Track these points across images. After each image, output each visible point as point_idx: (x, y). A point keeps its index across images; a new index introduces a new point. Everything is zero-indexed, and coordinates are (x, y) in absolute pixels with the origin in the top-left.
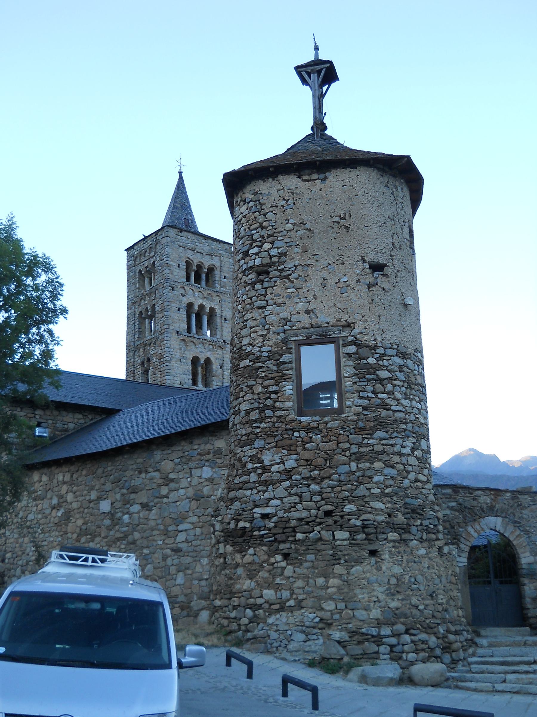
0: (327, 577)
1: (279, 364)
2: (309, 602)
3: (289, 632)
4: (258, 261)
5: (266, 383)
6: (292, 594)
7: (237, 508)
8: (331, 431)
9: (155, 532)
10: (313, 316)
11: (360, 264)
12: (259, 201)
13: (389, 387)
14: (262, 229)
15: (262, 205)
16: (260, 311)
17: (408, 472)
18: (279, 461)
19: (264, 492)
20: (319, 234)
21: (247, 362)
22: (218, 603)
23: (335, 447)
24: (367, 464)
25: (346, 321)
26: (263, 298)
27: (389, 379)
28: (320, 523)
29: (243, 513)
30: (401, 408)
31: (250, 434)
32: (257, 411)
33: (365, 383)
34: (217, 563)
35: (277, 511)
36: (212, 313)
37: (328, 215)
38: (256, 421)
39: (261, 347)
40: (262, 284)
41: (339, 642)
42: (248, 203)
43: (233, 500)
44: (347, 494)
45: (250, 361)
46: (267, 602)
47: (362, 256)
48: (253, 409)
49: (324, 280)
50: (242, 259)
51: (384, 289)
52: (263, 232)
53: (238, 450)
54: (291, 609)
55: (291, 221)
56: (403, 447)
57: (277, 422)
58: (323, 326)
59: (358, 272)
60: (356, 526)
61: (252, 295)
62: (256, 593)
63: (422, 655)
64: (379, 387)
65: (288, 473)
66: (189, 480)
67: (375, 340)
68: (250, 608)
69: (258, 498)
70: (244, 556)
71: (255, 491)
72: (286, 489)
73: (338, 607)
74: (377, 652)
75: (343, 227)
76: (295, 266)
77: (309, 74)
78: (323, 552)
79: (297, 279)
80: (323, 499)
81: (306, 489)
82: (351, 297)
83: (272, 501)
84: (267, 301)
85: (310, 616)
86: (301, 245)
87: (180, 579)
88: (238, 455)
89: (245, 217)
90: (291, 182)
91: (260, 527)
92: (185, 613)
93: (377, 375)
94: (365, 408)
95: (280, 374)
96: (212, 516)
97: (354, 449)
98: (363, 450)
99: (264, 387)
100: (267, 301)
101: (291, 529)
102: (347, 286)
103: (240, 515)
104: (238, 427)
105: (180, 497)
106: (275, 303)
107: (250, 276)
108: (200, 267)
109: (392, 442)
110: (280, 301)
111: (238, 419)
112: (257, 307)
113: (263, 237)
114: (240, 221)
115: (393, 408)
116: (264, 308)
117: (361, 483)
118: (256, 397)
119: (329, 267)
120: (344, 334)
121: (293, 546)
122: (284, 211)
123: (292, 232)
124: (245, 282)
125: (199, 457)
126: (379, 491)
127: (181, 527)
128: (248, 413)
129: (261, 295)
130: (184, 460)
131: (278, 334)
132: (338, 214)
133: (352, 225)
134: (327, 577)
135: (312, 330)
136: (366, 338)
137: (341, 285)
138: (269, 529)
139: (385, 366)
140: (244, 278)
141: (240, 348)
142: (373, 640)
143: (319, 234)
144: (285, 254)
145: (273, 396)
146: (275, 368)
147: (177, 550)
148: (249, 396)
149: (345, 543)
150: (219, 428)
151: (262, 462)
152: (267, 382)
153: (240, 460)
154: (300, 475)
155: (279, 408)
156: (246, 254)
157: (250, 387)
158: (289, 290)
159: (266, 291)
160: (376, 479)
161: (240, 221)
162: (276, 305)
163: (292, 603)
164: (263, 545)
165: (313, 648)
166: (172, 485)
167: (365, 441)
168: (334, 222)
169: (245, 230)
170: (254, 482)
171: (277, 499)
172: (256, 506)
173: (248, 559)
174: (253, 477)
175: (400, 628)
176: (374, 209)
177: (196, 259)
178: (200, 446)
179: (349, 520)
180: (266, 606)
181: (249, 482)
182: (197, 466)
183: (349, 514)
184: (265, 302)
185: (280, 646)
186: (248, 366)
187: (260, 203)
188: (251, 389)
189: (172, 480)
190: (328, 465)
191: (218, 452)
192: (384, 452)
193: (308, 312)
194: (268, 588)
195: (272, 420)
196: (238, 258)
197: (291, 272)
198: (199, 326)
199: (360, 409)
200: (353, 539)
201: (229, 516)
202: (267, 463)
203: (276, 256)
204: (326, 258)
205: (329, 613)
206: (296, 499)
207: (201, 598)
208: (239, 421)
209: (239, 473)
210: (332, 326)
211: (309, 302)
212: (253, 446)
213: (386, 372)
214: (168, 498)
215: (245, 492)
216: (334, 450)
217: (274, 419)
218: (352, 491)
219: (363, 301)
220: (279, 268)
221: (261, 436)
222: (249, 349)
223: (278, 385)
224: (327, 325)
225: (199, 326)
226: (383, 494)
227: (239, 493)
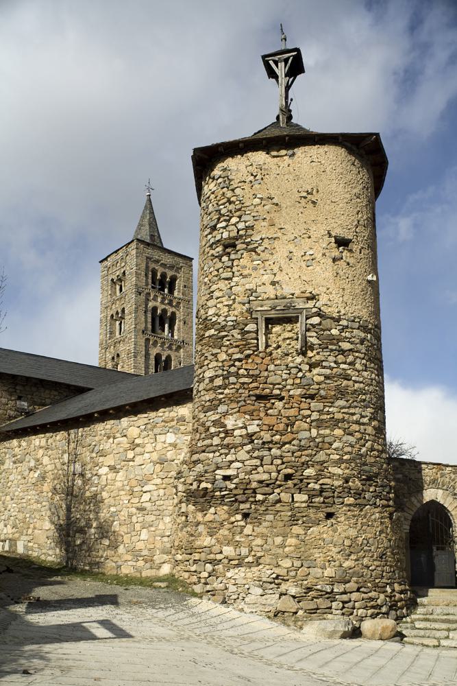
0: (285, 536)
1: (243, 333)
2: (267, 559)
3: (247, 586)
4: (225, 235)
5: (230, 351)
6: (250, 551)
7: (199, 470)
8: (293, 398)
9: (122, 493)
11: (326, 238)
12: (228, 177)
14: (230, 204)
15: (230, 180)
16: (227, 282)
18: (241, 425)
19: (226, 455)
20: (286, 208)
21: (212, 332)
22: (179, 557)
23: (297, 414)
24: (328, 431)
25: (311, 293)
26: (229, 270)
27: (350, 350)
28: (280, 486)
29: (206, 475)
30: (361, 379)
31: (213, 400)
32: (221, 378)
33: (328, 353)
34: (178, 521)
35: (238, 474)
37: (295, 190)
38: (219, 387)
39: (226, 317)
40: (229, 257)
41: (294, 597)
42: (217, 180)
43: (196, 462)
44: (308, 459)
45: (216, 330)
46: (226, 558)
48: (217, 376)
50: (209, 234)
51: (348, 264)
52: (231, 207)
53: (202, 415)
54: (250, 565)
55: (258, 196)
56: (362, 417)
57: (240, 388)
59: (324, 246)
60: (314, 490)
62: (216, 549)
63: (370, 612)
64: (341, 358)
65: (250, 437)
66: (154, 445)
67: (339, 312)
68: (210, 563)
69: (219, 460)
70: (206, 514)
71: (217, 454)
72: (248, 452)
73: (295, 565)
74: (331, 608)
75: (310, 202)
76: (261, 239)
77: (276, 63)
78: (282, 513)
79: (263, 251)
80: (283, 463)
81: (267, 453)
82: (316, 270)
83: (234, 464)
84: (233, 273)
85: (266, 572)
86: (268, 218)
87: (144, 535)
88: (201, 421)
89: (213, 193)
90: (259, 157)
91: (222, 488)
92: (148, 565)
93: (340, 347)
94: (327, 377)
95: (245, 342)
96: (175, 478)
97: (315, 416)
98: (325, 417)
101: (252, 490)
102: (312, 260)
103: (202, 476)
104: (202, 393)
105: (145, 462)
107: (217, 250)
109: (352, 411)
110: (245, 272)
111: (202, 386)
112: (223, 279)
114: (209, 197)
115: (353, 378)
116: (230, 279)
117: (322, 449)
118: (220, 364)
120: (307, 306)
121: (253, 506)
123: (259, 208)
124: (213, 255)
125: (163, 424)
126: (338, 457)
127: (144, 489)
128: (212, 380)
129: (228, 267)
130: (149, 426)
131: (244, 304)
132: (306, 190)
133: (319, 200)
134: (285, 536)
135: (276, 301)
136: (330, 309)
137: (307, 259)
138: (231, 490)
139: (348, 338)
140: (212, 252)
141: (206, 318)
142: (327, 596)
143: (286, 208)
144: (252, 228)
146: (239, 337)
147: (141, 509)
148: (214, 364)
149: (304, 505)
150: (182, 397)
151: (225, 426)
152: (232, 350)
153: (203, 425)
154: (262, 439)
156: (214, 228)
157: (215, 355)
158: (255, 263)
159: (233, 264)
160: (335, 445)
161: (209, 197)
163: (250, 559)
164: (223, 505)
165: (269, 602)
166: (138, 450)
167: (327, 409)
168: (301, 197)
169: (213, 205)
170: (217, 445)
171: (238, 461)
172: (218, 468)
173: (209, 517)
174: (216, 441)
175: (352, 585)
176: (341, 186)
178: (164, 413)
179: (309, 483)
180: (226, 561)
181: (212, 445)
182: (162, 432)
183: (308, 477)
184: (231, 273)
185: (238, 598)
186: (213, 335)
188: (216, 357)
189: (138, 445)
190: (289, 430)
191: (182, 420)
192: (343, 420)
193: (273, 283)
194: (228, 544)
195: (236, 386)
196: (206, 233)
199: (322, 378)
200: (311, 502)
201: (192, 477)
202: (229, 427)
203: (243, 229)
204: (293, 231)
205: (286, 570)
206: (257, 462)
207: (163, 552)
208: (203, 388)
209: (202, 437)
210: (297, 298)
213: (349, 344)
214: (134, 461)
215: (208, 454)
216: (295, 417)
217: (237, 386)
218: (311, 455)
219: (328, 274)
220: (246, 241)
221: (225, 402)
222: (214, 319)
223: (242, 353)
224: (291, 296)
226: (341, 461)
227: (202, 456)
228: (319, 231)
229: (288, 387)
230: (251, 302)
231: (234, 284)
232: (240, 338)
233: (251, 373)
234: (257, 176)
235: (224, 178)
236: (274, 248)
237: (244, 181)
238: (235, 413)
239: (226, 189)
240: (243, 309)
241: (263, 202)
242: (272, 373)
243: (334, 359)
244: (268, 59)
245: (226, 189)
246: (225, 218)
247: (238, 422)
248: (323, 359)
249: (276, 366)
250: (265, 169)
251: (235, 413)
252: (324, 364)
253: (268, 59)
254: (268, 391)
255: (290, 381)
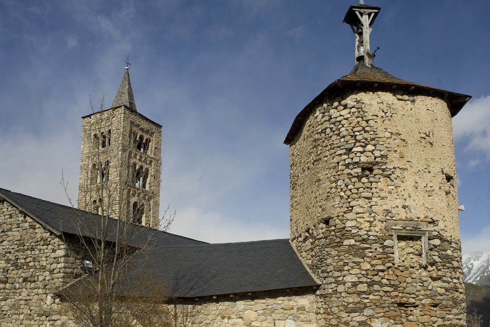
5: (374, 262)
10: (408, 211)
20: (411, 145)
25: (431, 218)
26: (369, 190)
31: (357, 303)
37: (417, 131)
38: (364, 292)
39: (368, 231)
42: (351, 108)
47: (442, 169)
49: (416, 183)
52: (366, 135)
53: (344, 315)
57: (384, 296)
58: (414, 220)
59: (440, 181)
61: (359, 187)
67: (451, 236)
75: (429, 143)
76: (394, 168)
79: (396, 179)
82: (435, 200)
94: (447, 290)
99: (372, 266)
100: (373, 194)
106: (379, 196)
110: (383, 194)
112: (364, 197)
113: (366, 139)
115: (460, 290)
118: (364, 272)
119: (419, 173)
122: (384, 121)
123: (391, 140)
128: (355, 285)
129: (367, 188)
131: (382, 222)
140: (347, 171)
143: (411, 145)
144: (386, 157)
145: (381, 274)
146: (381, 250)
155: (385, 284)
156: (349, 151)
157: (358, 263)
158: (390, 187)
162: (380, 198)
184: (371, 194)
187: (362, 110)
193: (404, 207)
197: (391, 173)
203: (379, 157)
204: (417, 165)
210: (421, 221)
211: (405, 199)
212: (362, 314)
217: (381, 293)
220: (382, 167)
223: (384, 265)
224: (417, 219)
228: (435, 168)
229: (421, 297)
230: (387, 221)
231: (374, 204)
232: (382, 251)
233: (392, 283)
234: (388, 114)
235: (358, 108)
236: (404, 177)
237: (376, 115)
238: (381, 317)
239: (360, 119)
240: (382, 226)
241: (393, 137)
242: (410, 285)
243: (450, 275)
244: (355, 9)
245: (360, 119)
246: (362, 144)
247: (383, 324)
248: (444, 275)
249: (412, 278)
250: (393, 108)
251: (381, 317)
252: (444, 278)
253: (355, 9)
254: (405, 299)
255: (422, 292)
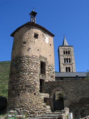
13: (24, 64)
17: (26, 79)
36: (70, 59)
108: (67, 51)
177: (65, 50)
192: (22, 76)
198: (67, 62)
225: (67, 62)
